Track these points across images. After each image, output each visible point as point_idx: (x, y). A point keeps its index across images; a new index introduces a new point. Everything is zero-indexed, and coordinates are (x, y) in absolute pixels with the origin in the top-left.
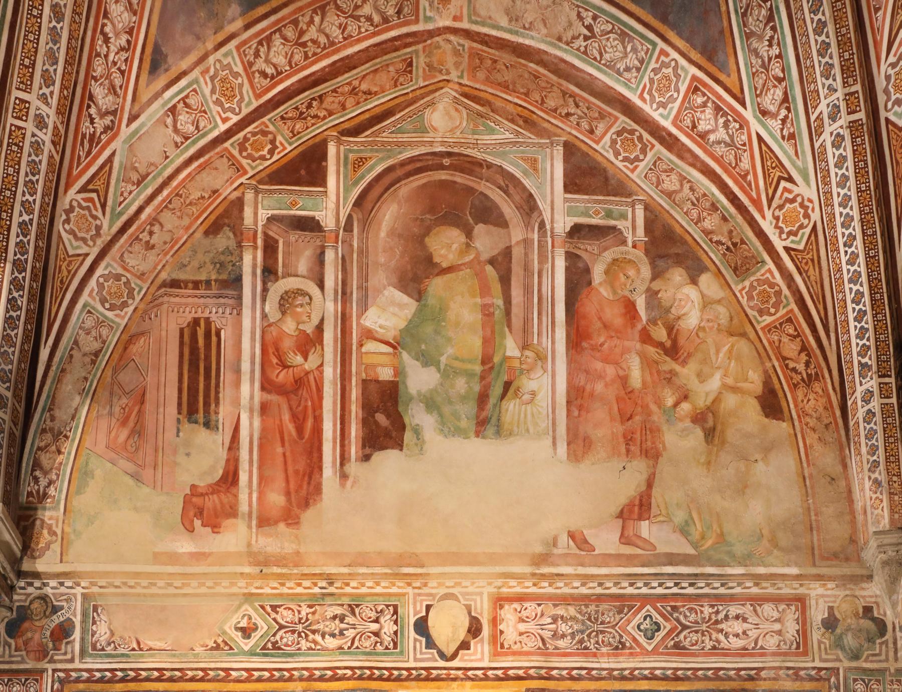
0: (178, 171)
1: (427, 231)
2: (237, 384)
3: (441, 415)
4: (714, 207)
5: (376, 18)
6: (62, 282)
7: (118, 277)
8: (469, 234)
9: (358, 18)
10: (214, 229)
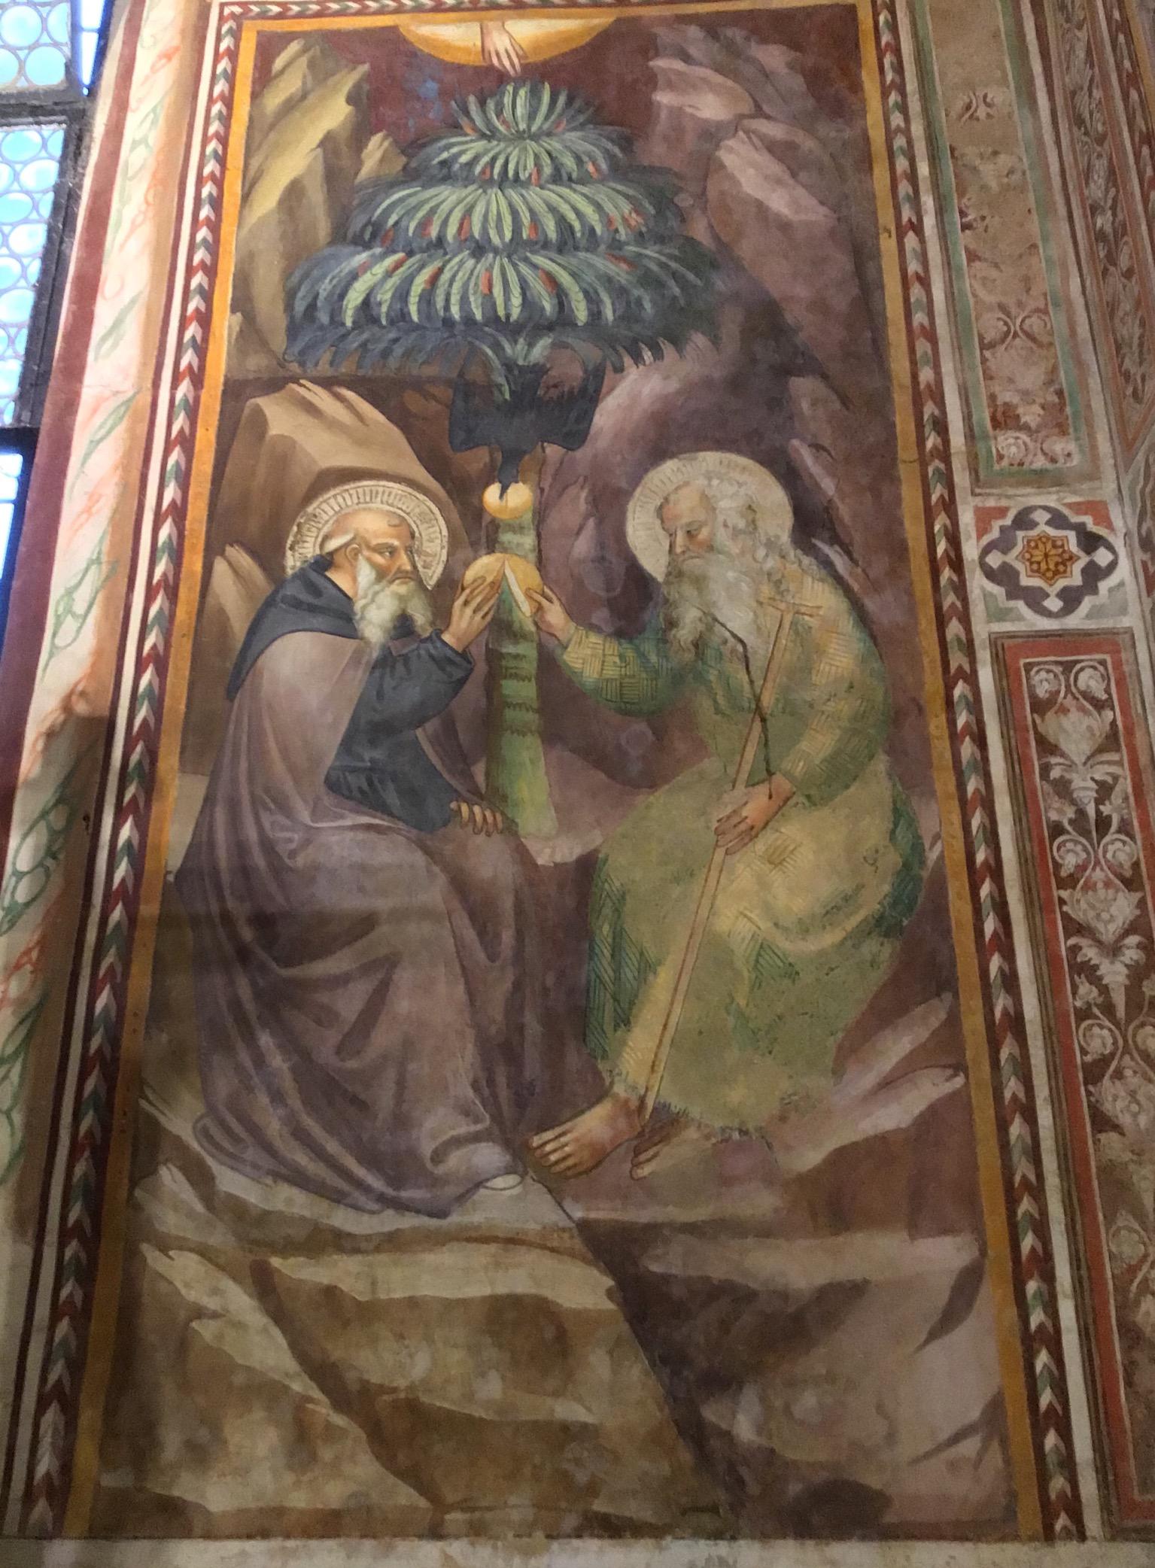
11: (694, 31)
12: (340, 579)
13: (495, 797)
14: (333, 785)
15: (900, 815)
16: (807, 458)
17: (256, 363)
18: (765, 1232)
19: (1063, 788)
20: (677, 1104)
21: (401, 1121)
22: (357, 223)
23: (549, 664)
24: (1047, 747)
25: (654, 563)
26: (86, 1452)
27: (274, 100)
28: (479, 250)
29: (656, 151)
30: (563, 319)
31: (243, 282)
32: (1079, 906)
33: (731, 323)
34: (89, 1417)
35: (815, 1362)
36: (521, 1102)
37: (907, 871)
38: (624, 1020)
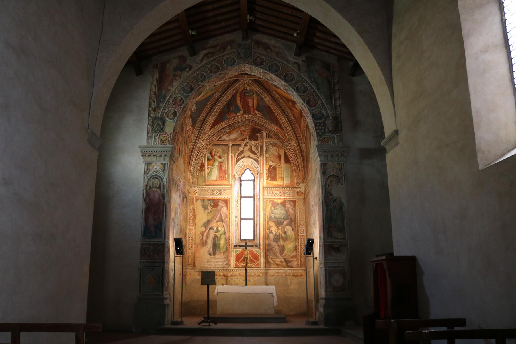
11: (288, 201)
12: (273, 231)
13: (279, 242)
14: (273, 241)
15: (295, 243)
16: (293, 226)
17: (268, 220)
18: (290, 258)
19: (302, 242)
20: (286, 254)
21: (277, 254)
22: (272, 212)
23: (282, 236)
24: (301, 240)
25: (286, 231)
26: (266, 265)
27: (268, 204)
28: (278, 214)
29: (286, 209)
30: (282, 218)
31: (267, 215)
32: (302, 247)
33: (289, 219)
34: (266, 264)
35: (291, 262)
36: (281, 254)
37: (296, 245)
38: (285, 251)
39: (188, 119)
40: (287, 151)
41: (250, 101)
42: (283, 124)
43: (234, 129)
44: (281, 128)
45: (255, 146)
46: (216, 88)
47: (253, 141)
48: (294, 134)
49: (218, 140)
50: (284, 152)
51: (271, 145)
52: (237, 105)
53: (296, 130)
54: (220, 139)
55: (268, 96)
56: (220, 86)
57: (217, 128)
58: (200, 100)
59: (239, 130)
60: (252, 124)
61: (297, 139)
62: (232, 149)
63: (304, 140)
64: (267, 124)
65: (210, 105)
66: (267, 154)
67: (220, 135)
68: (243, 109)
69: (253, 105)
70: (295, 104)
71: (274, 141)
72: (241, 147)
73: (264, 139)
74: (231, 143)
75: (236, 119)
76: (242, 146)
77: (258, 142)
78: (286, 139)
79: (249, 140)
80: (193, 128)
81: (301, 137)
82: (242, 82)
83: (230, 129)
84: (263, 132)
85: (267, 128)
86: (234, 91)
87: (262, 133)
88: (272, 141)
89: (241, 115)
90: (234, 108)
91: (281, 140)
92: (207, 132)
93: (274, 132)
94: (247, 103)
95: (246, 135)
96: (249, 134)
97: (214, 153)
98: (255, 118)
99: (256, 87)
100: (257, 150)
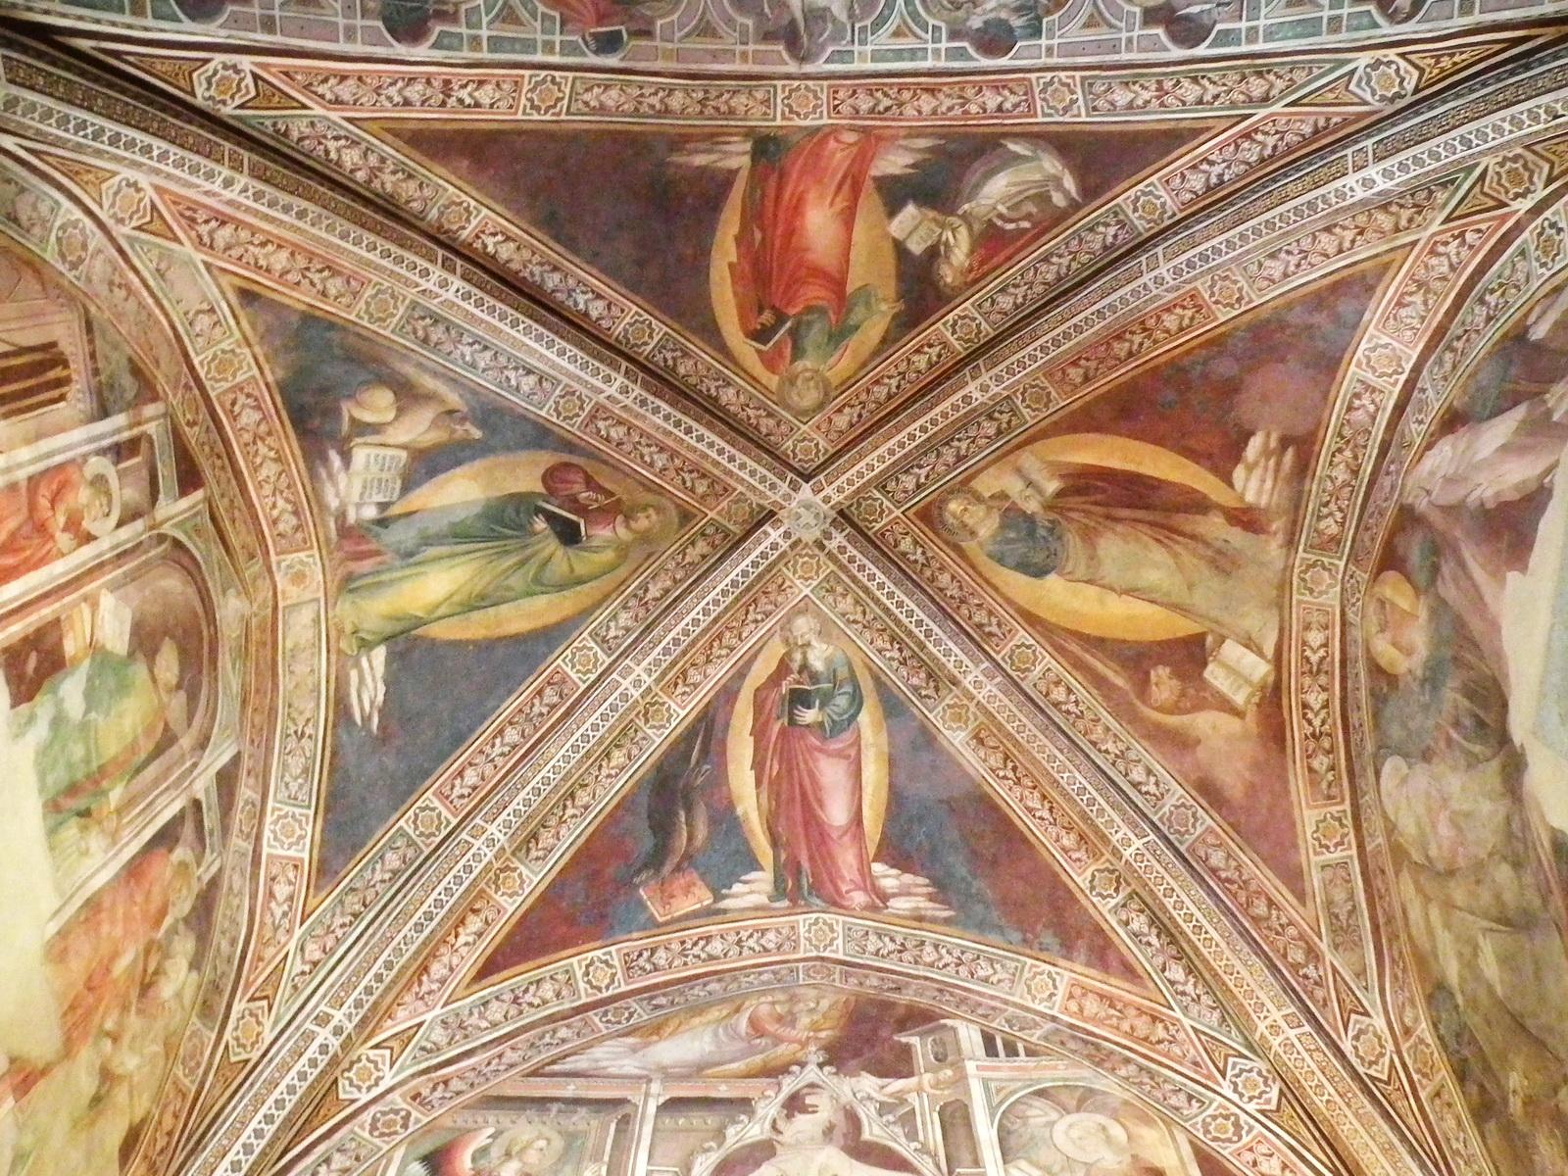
0: (167, 315)
1: (172, 637)
2: (28, 441)
3: (51, 743)
4: (233, 942)
5: (275, 513)
6: (77, 173)
7: (84, 247)
8: (179, 686)
9: (274, 494)
10: (136, 371)
39: (296, 764)
40: (1215, 1139)
41: (831, 774)
42: (1127, 923)
43: (697, 1009)
44: (1105, 967)
45: (883, 1109)
46: (580, 581)
47: (864, 1073)
48: (1241, 944)
49: (535, 1073)
50: (1187, 1151)
51: (1038, 1103)
52: (731, 807)
53: (1255, 920)
54: (556, 1068)
55: (977, 666)
56: (612, 567)
57: (548, 990)
58: (439, 631)
59: (737, 1010)
60: (853, 980)
61: (1289, 989)
62: (655, 1130)
63: (1361, 974)
64: (981, 973)
65: (512, 735)
66: (1023, 1164)
67: (564, 1041)
68: (776, 858)
69: (857, 819)
70: (1205, 664)
71: (1070, 1073)
72: (751, 1113)
73: (970, 1067)
74: (655, 1087)
75: (716, 947)
76: (760, 1112)
77: (912, 1082)
78: (1176, 1050)
79: (827, 1069)
80: (325, 870)
81: (1328, 957)
82: (774, 546)
83: (657, 1007)
84: (942, 1021)
85: (980, 1005)
86: (710, 670)
87: (945, 1026)
88: (1048, 1074)
89: (756, 908)
90: (702, 832)
91: (1132, 1068)
92: (443, 982)
93: (1049, 1026)
94: (804, 795)
95: (804, 1044)
96: (823, 1035)
97: (474, 1159)
98: (873, 943)
99: (881, 586)
100: (912, 1135)
